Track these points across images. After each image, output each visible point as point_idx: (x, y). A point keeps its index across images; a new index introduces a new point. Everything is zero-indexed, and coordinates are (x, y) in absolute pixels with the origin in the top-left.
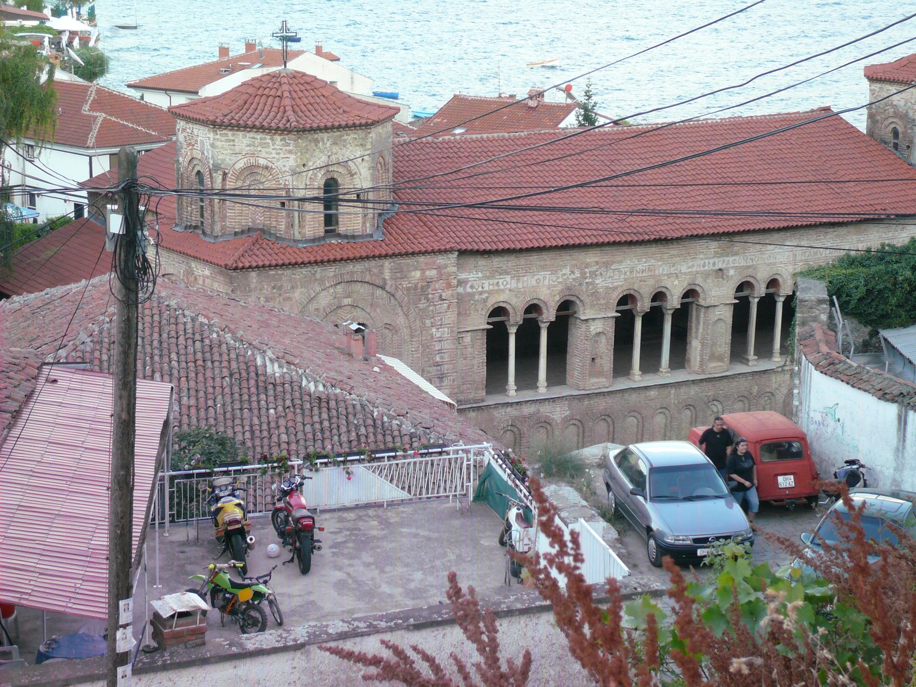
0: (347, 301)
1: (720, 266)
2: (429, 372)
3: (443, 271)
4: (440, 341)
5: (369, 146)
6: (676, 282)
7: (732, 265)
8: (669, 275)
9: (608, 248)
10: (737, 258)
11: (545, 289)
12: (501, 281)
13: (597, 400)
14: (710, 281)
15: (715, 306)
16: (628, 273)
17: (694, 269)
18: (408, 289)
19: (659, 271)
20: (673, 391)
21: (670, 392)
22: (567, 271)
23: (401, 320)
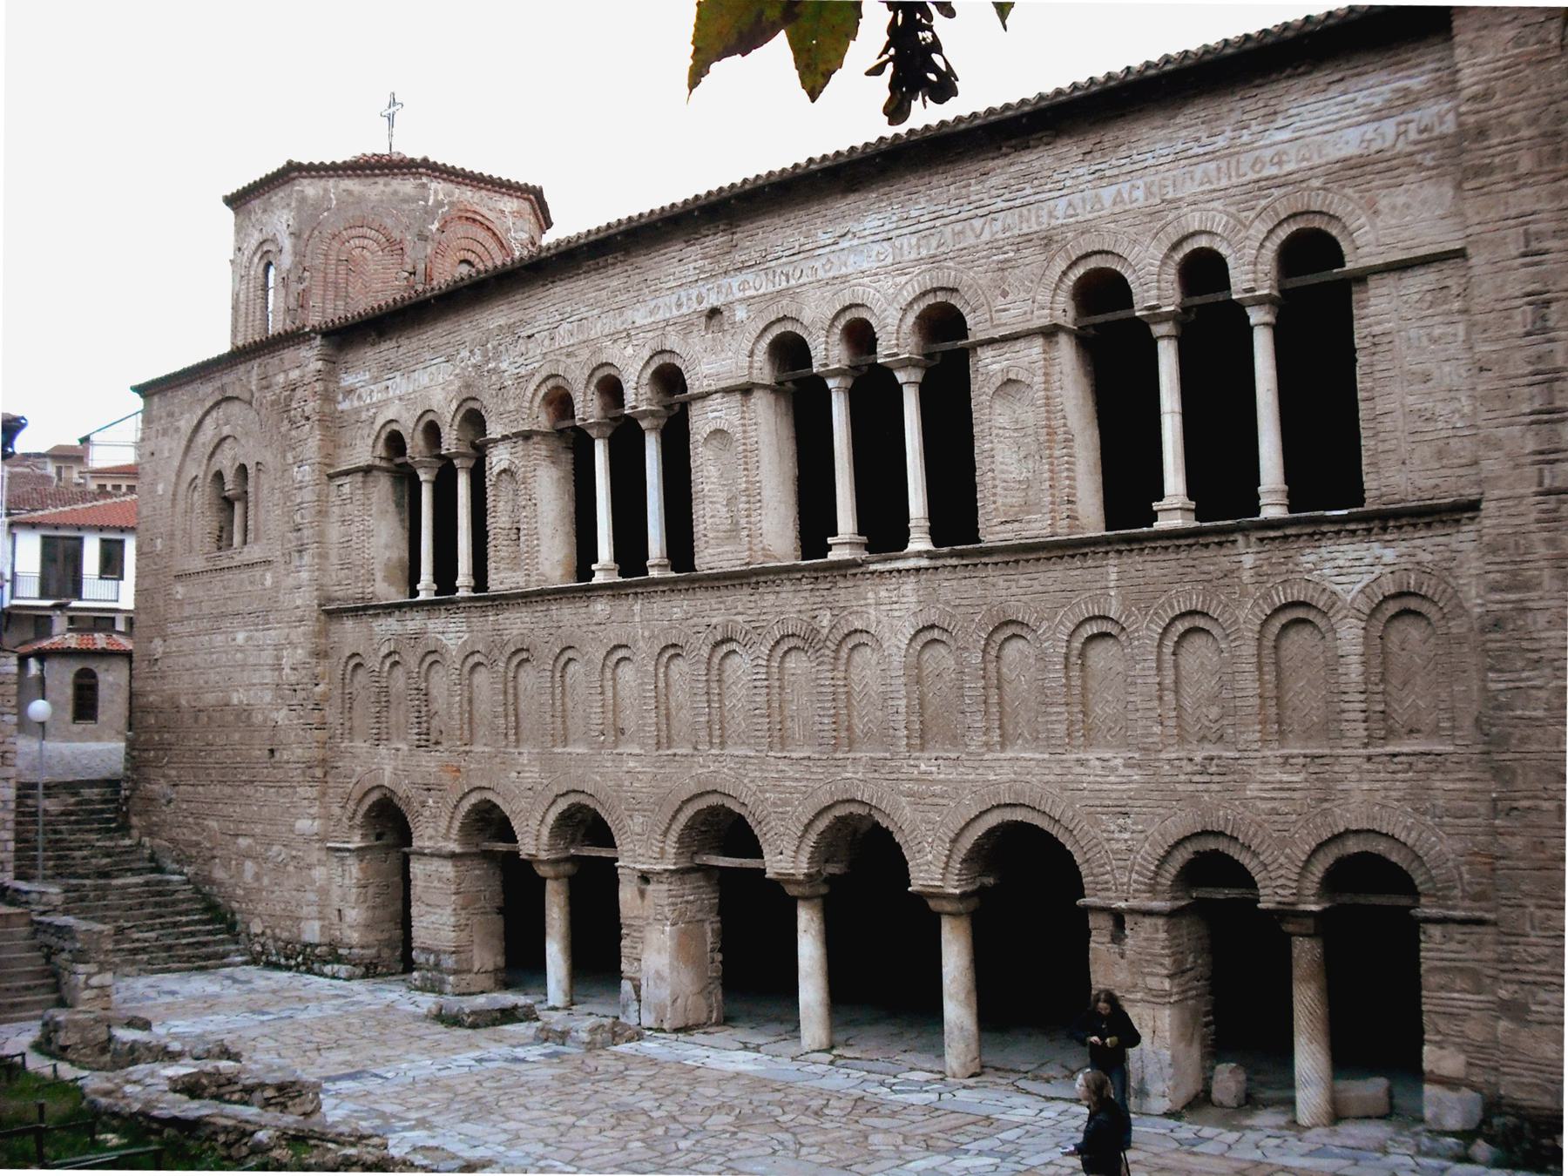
0: (226, 430)
1: (713, 300)
2: (290, 541)
3: (307, 369)
4: (300, 488)
5: (293, 204)
6: (630, 350)
7: (740, 295)
8: (614, 337)
9: (518, 297)
10: (748, 276)
11: (439, 388)
12: (389, 383)
13: (507, 614)
14: (694, 339)
15: (705, 396)
16: (547, 342)
17: (659, 317)
18: (273, 403)
19: (597, 329)
20: (637, 607)
21: (630, 608)
22: (465, 353)
23: (268, 457)
